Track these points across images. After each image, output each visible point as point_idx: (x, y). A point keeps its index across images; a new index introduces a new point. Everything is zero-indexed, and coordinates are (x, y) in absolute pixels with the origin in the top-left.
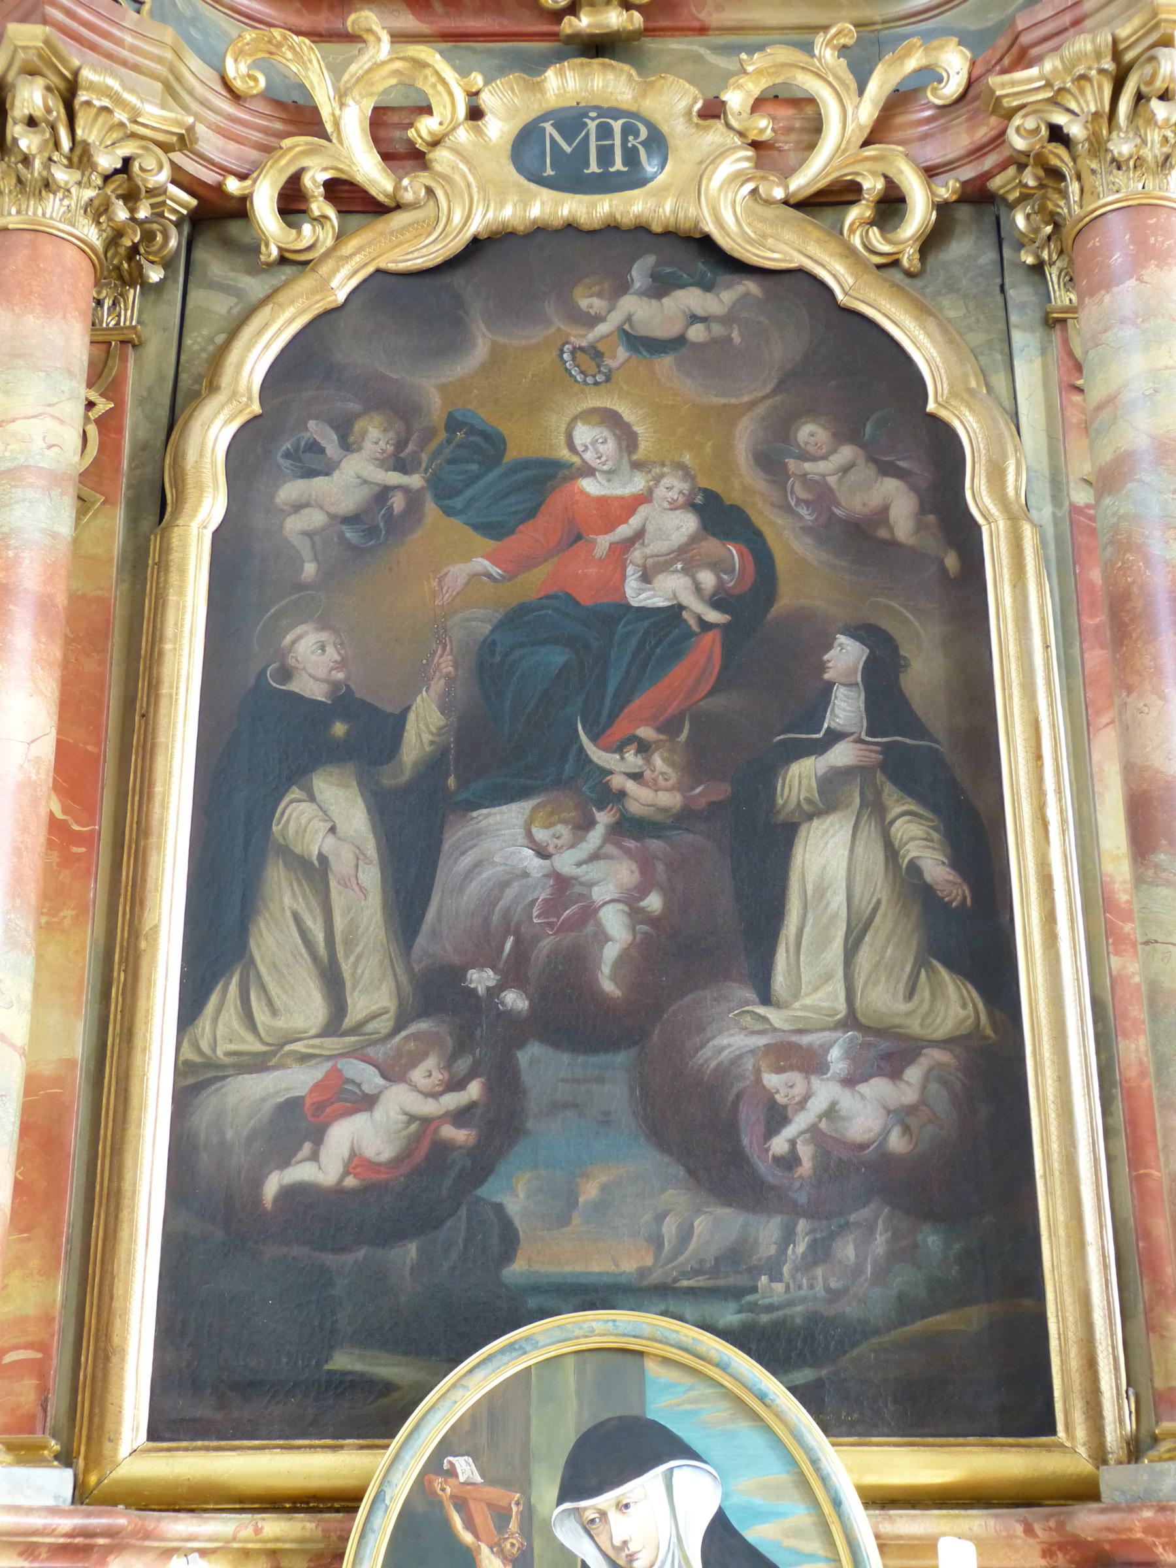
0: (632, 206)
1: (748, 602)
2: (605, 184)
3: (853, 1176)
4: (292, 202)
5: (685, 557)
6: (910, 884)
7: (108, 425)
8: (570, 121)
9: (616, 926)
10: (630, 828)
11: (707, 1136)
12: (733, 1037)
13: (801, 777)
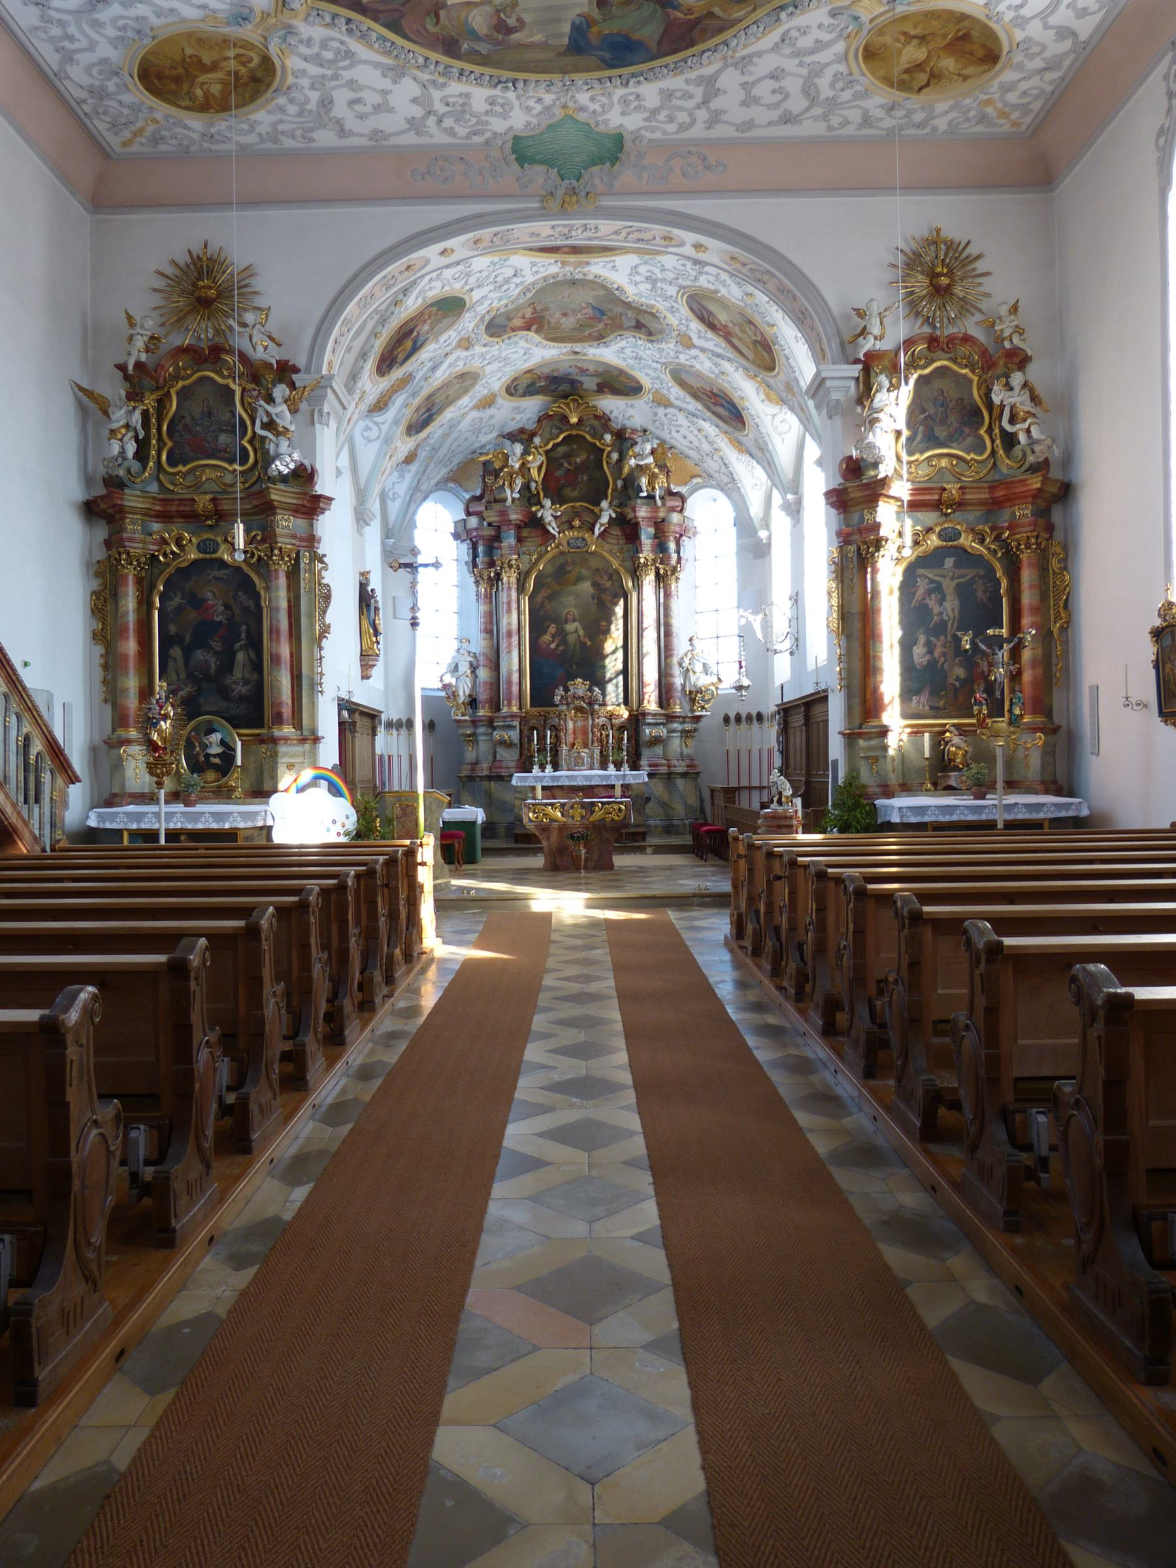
0: (214, 556)
1: (231, 620)
2: (210, 553)
3: (242, 698)
4: (165, 555)
5: (222, 613)
6: (251, 660)
7: (142, 592)
8: (204, 541)
9: (213, 666)
10: (216, 653)
11: (224, 693)
12: (228, 681)
13: (238, 645)
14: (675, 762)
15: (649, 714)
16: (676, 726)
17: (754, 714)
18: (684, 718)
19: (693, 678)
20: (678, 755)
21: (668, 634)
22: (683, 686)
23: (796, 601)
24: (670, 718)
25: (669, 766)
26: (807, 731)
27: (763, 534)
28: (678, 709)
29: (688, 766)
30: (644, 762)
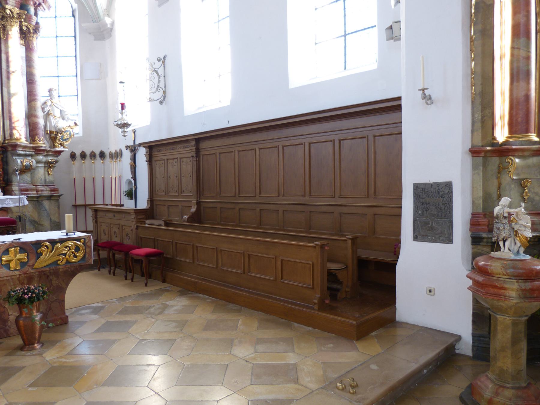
14: (40, 187)
15: (20, 146)
16: (41, 158)
17: (97, 153)
18: (48, 151)
19: (53, 121)
20: (43, 181)
21: (30, 81)
22: (45, 127)
23: (164, 62)
24: (38, 151)
25: (37, 191)
26: (198, 162)
27: (108, 21)
28: (43, 144)
29: (51, 190)
30: (15, 188)
